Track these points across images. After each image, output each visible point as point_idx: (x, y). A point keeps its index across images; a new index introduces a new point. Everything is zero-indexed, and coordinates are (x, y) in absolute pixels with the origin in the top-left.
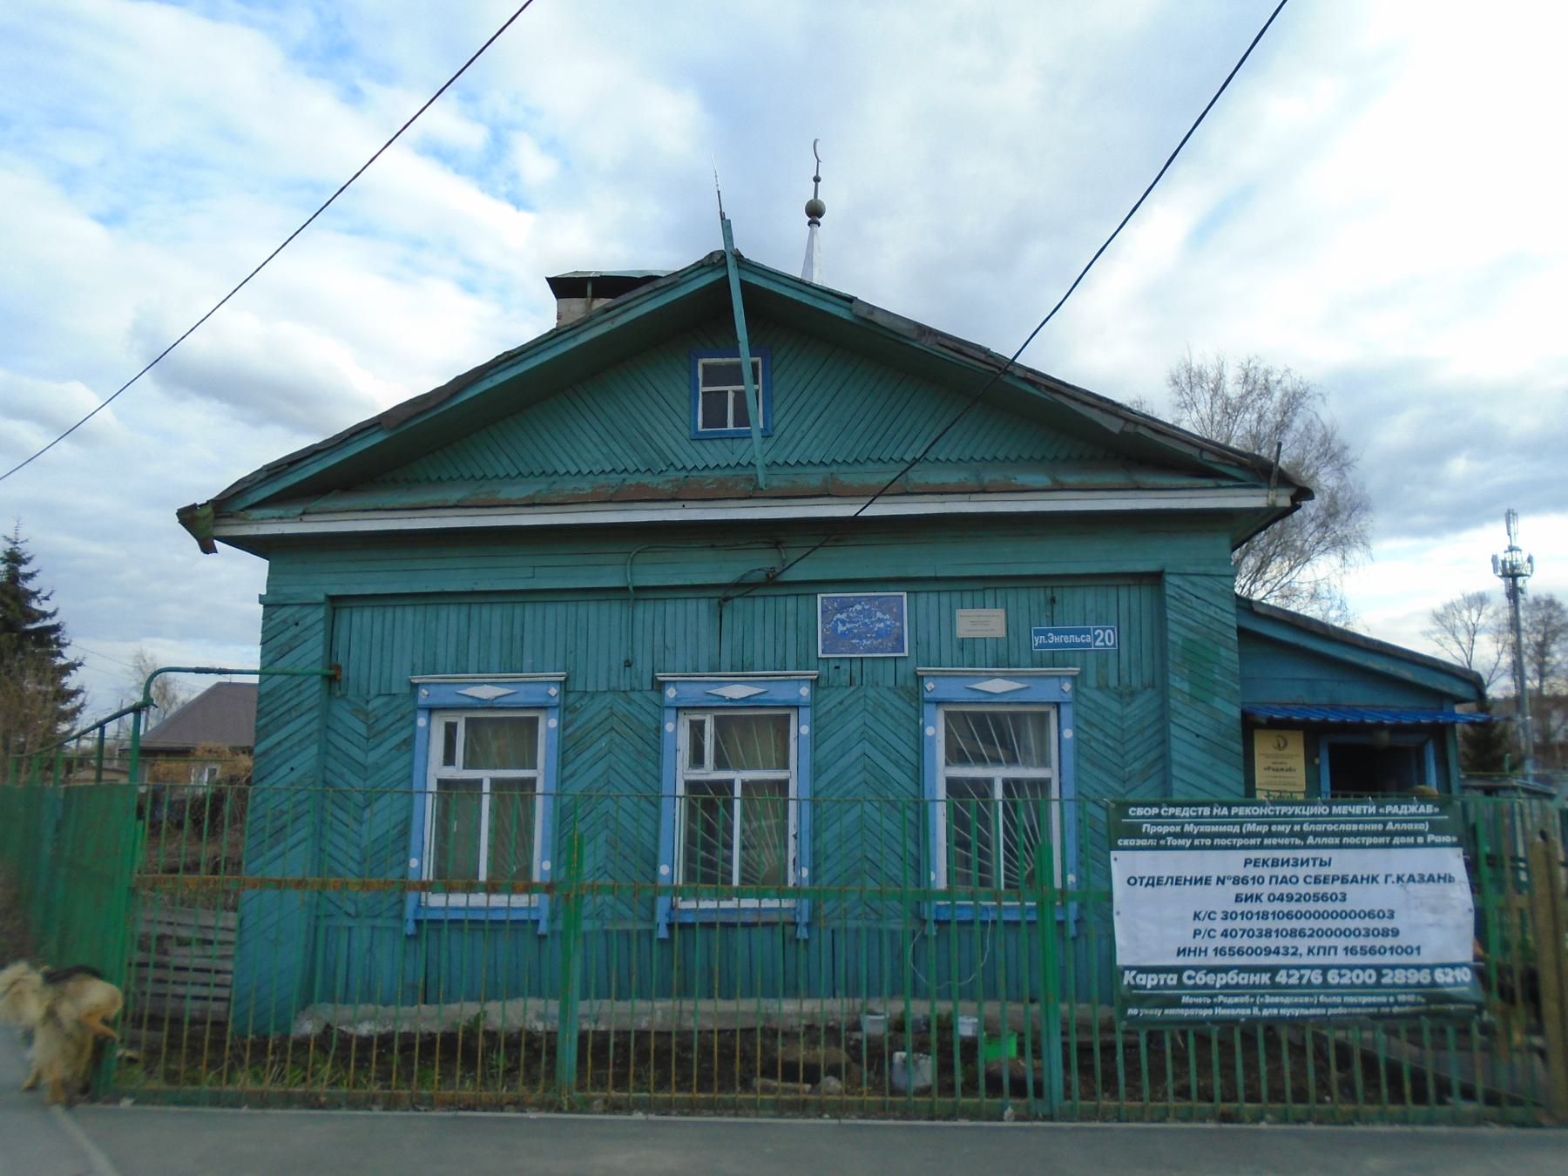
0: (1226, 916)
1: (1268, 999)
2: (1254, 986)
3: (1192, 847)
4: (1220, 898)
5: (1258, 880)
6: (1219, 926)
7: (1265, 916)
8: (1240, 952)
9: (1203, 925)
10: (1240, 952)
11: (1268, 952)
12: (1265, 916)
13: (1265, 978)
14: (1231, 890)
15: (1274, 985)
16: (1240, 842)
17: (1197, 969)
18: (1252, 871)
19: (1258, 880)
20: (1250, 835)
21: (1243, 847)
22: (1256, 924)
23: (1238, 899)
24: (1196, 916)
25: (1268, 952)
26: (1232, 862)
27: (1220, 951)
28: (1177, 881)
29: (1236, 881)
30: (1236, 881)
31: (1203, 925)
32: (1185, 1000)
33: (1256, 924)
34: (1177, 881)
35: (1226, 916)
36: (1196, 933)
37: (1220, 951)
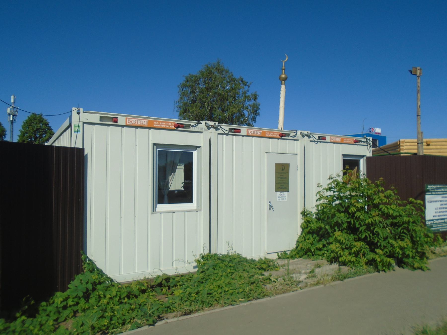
0: (440, 208)
1: (444, 225)
2: (442, 223)
3: (436, 194)
4: (438, 205)
5: (443, 201)
6: (439, 210)
7: (444, 208)
8: (440, 216)
9: (437, 210)
10: (440, 216)
11: (444, 215)
12: (444, 208)
13: (443, 221)
14: (440, 203)
15: (445, 222)
16: (441, 193)
17: (435, 220)
18: (442, 199)
19: (443, 201)
20: (443, 192)
21: (442, 194)
22: (443, 210)
23: (441, 205)
24: (436, 209)
25: (444, 215)
26: (439, 198)
27: (439, 216)
28: (434, 201)
29: (441, 201)
30: (441, 201)
31: (437, 210)
32: (434, 226)
33: (443, 210)
34: (434, 201)
35: (440, 208)
36: (436, 212)
37: (439, 216)
